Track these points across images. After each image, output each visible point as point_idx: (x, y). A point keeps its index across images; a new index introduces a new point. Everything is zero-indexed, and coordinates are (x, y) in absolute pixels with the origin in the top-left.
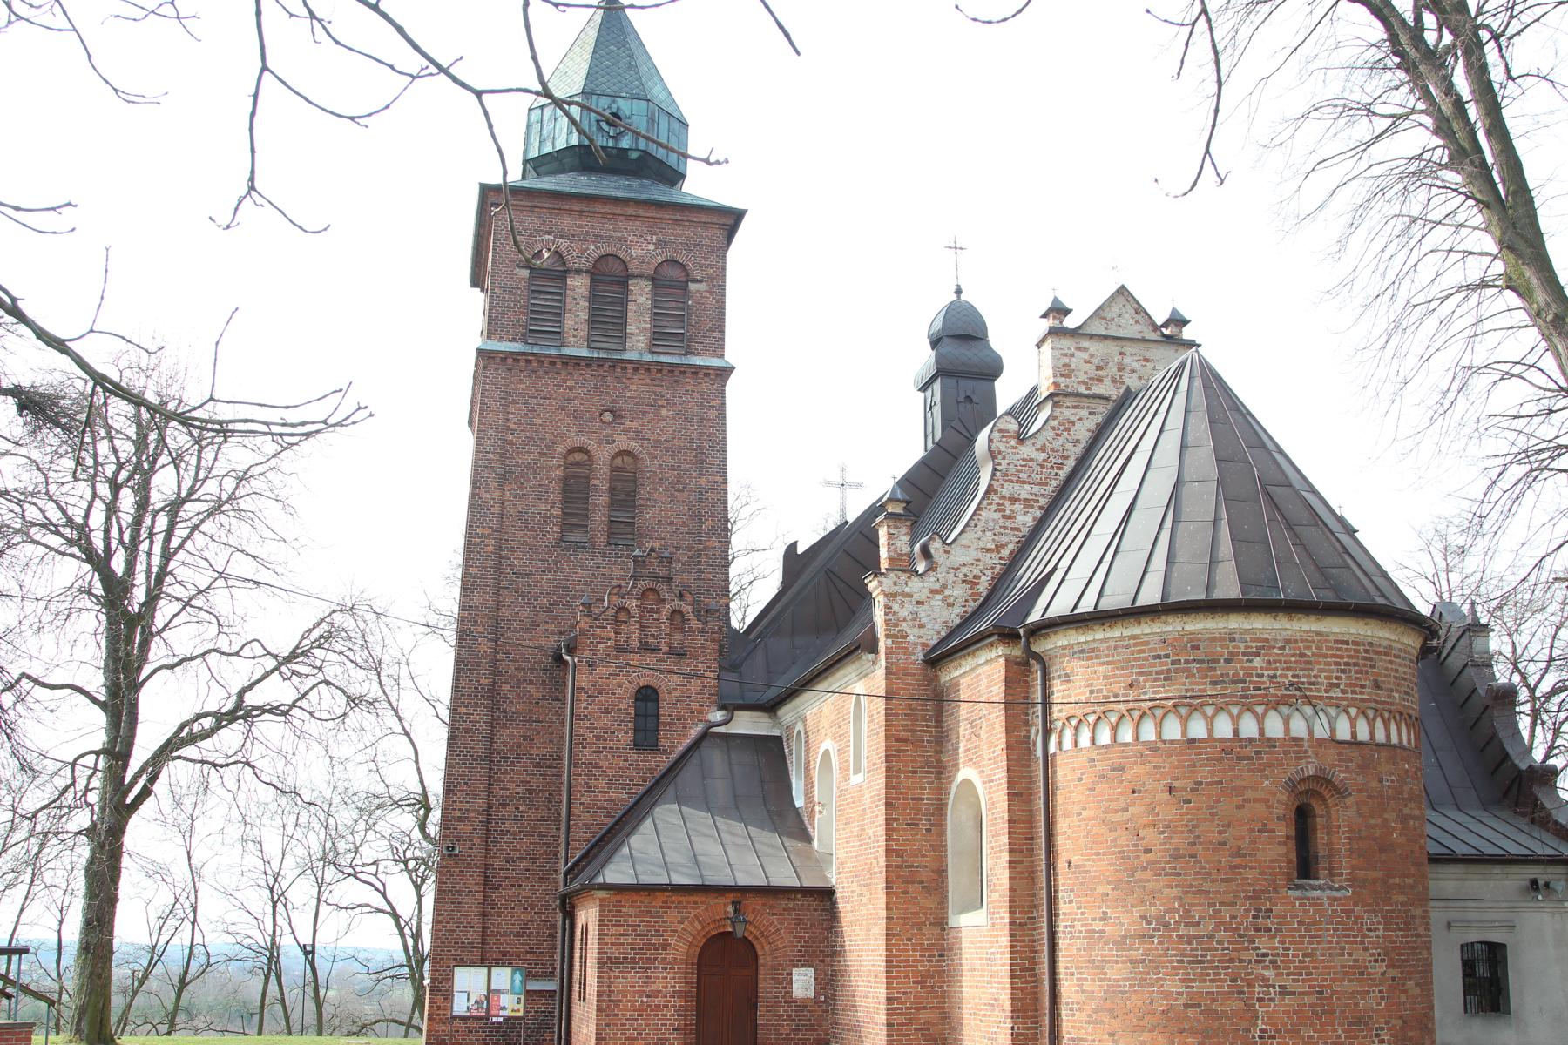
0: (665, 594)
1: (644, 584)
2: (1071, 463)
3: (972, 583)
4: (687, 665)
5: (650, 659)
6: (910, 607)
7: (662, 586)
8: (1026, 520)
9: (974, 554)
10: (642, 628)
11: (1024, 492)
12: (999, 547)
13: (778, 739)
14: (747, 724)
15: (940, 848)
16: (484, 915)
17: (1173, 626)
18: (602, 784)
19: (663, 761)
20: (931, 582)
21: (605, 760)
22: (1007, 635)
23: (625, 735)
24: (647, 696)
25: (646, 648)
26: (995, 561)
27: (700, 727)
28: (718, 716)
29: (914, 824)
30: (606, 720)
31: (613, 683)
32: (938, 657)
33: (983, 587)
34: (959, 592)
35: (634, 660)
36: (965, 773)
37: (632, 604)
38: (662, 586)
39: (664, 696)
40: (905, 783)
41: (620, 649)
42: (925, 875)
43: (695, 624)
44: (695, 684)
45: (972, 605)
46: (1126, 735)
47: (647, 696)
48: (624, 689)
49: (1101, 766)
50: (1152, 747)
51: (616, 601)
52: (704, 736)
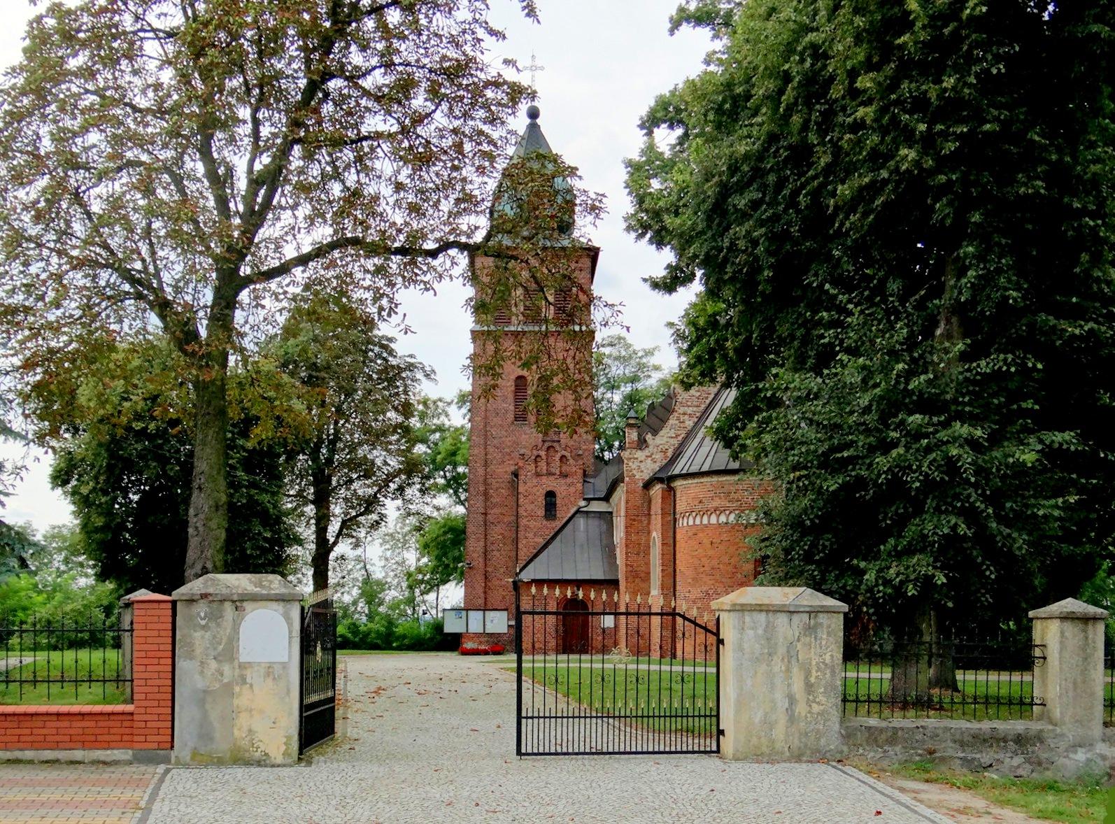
0: (558, 448)
1: (547, 445)
2: (712, 396)
3: (665, 452)
4: (569, 480)
5: (551, 478)
6: (637, 463)
7: (555, 444)
8: (689, 423)
9: (665, 439)
10: (548, 464)
11: (689, 410)
12: (677, 436)
13: (611, 513)
14: (597, 507)
15: (648, 564)
16: (485, 593)
17: (715, 479)
18: (531, 535)
19: (558, 524)
20: (647, 452)
21: (532, 524)
22: (661, 480)
23: (541, 512)
24: (550, 495)
25: (550, 474)
26: (676, 442)
27: (575, 509)
28: (583, 503)
29: (638, 554)
30: (532, 506)
31: (535, 489)
32: (648, 485)
33: (670, 454)
34: (658, 456)
35: (544, 479)
36: (654, 534)
37: (543, 453)
38: (555, 444)
39: (558, 495)
40: (634, 537)
41: (538, 475)
42: (643, 575)
43: (571, 461)
44: (572, 489)
45: (665, 462)
46: (698, 522)
47: (550, 495)
48: (540, 493)
49: (690, 534)
50: (706, 526)
51: (535, 453)
52: (578, 512)
